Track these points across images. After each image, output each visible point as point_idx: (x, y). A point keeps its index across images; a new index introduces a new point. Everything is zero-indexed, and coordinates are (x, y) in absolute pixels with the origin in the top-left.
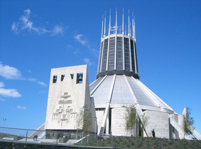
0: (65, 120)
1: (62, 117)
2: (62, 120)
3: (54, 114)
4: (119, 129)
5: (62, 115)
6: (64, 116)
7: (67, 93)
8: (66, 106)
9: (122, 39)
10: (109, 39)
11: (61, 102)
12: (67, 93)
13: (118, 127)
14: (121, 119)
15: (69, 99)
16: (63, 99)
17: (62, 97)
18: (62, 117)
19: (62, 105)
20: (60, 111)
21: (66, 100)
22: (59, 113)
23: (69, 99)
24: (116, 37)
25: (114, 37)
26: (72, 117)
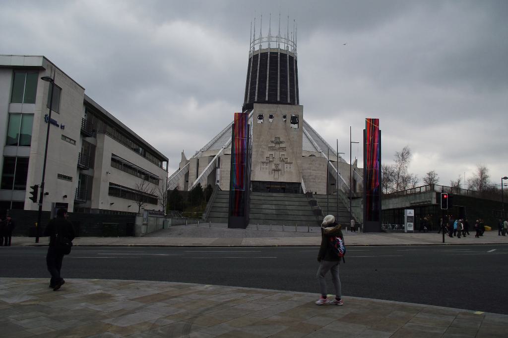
0: (278, 170)
1: (274, 167)
2: (274, 170)
3: (263, 163)
4: (314, 182)
5: (273, 165)
6: (277, 165)
7: (279, 138)
8: (277, 155)
9: (286, 57)
10: (269, 53)
11: (272, 148)
12: (279, 138)
13: (312, 180)
14: (315, 170)
15: (282, 145)
16: (274, 145)
17: (272, 142)
18: (274, 167)
19: (273, 153)
20: (271, 160)
21: (277, 146)
22: (269, 161)
23: (282, 145)
24: (279, 54)
25: (277, 53)
26: (287, 168)
